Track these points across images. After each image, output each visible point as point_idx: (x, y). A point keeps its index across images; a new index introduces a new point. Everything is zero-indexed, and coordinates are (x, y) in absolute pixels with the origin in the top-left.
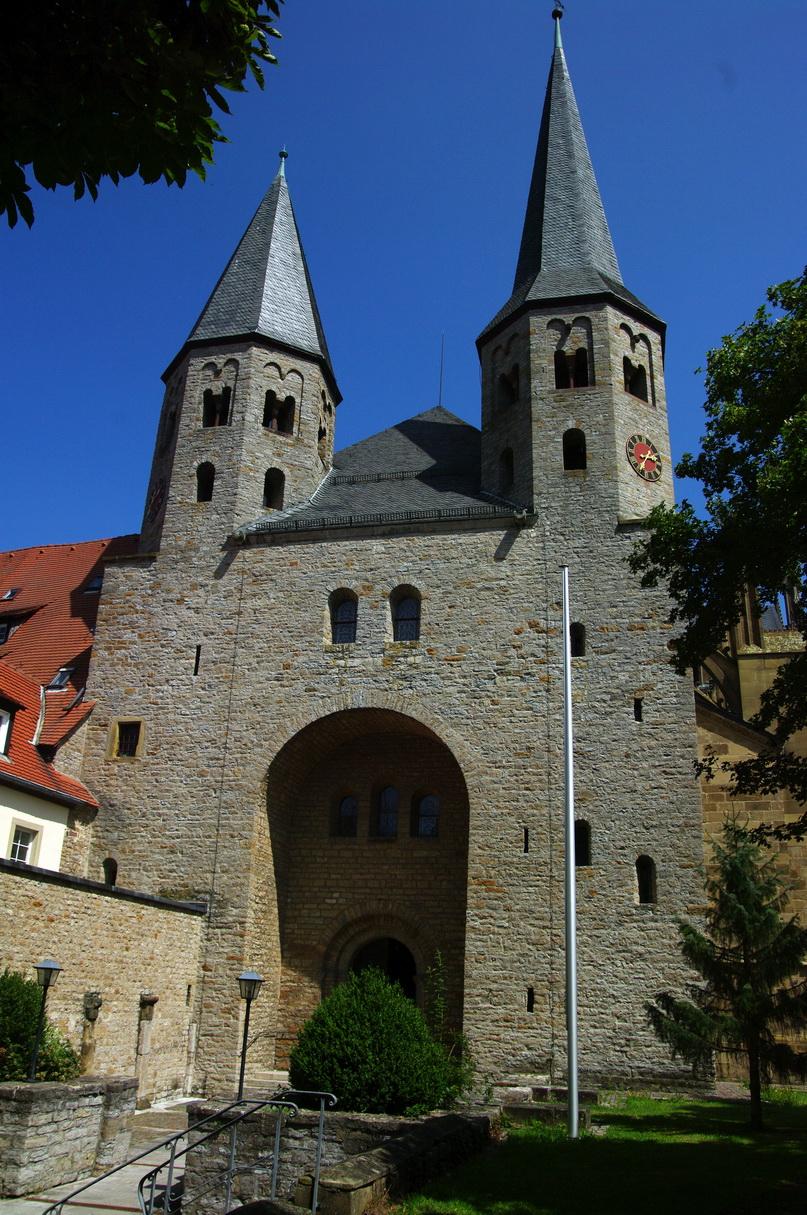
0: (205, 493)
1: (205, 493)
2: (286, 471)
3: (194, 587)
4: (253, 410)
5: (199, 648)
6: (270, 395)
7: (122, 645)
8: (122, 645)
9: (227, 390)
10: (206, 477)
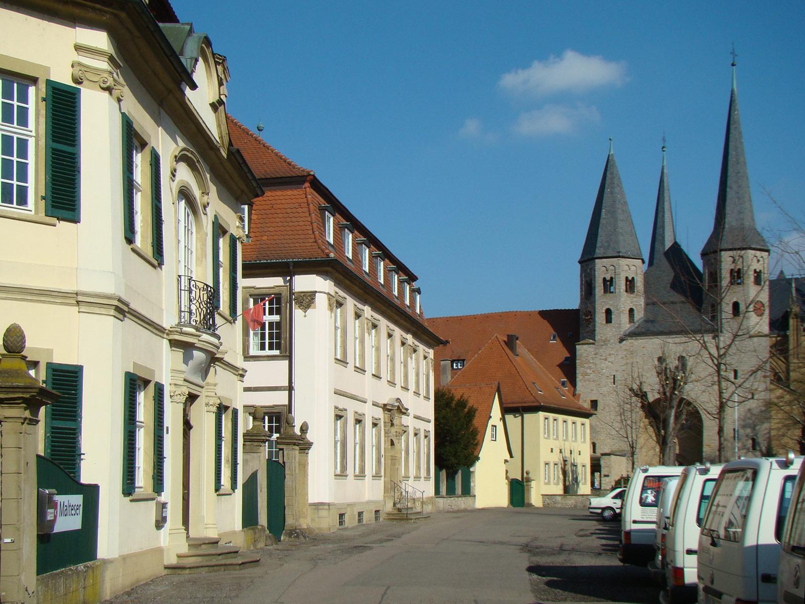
0: (609, 320)
1: (609, 320)
2: (634, 308)
3: (610, 355)
4: (621, 285)
5: (614, 376)
6: (627, 278)
7: (587, 374)
8: (587, 374)
9: (612, 278)
10: (608, 312)
